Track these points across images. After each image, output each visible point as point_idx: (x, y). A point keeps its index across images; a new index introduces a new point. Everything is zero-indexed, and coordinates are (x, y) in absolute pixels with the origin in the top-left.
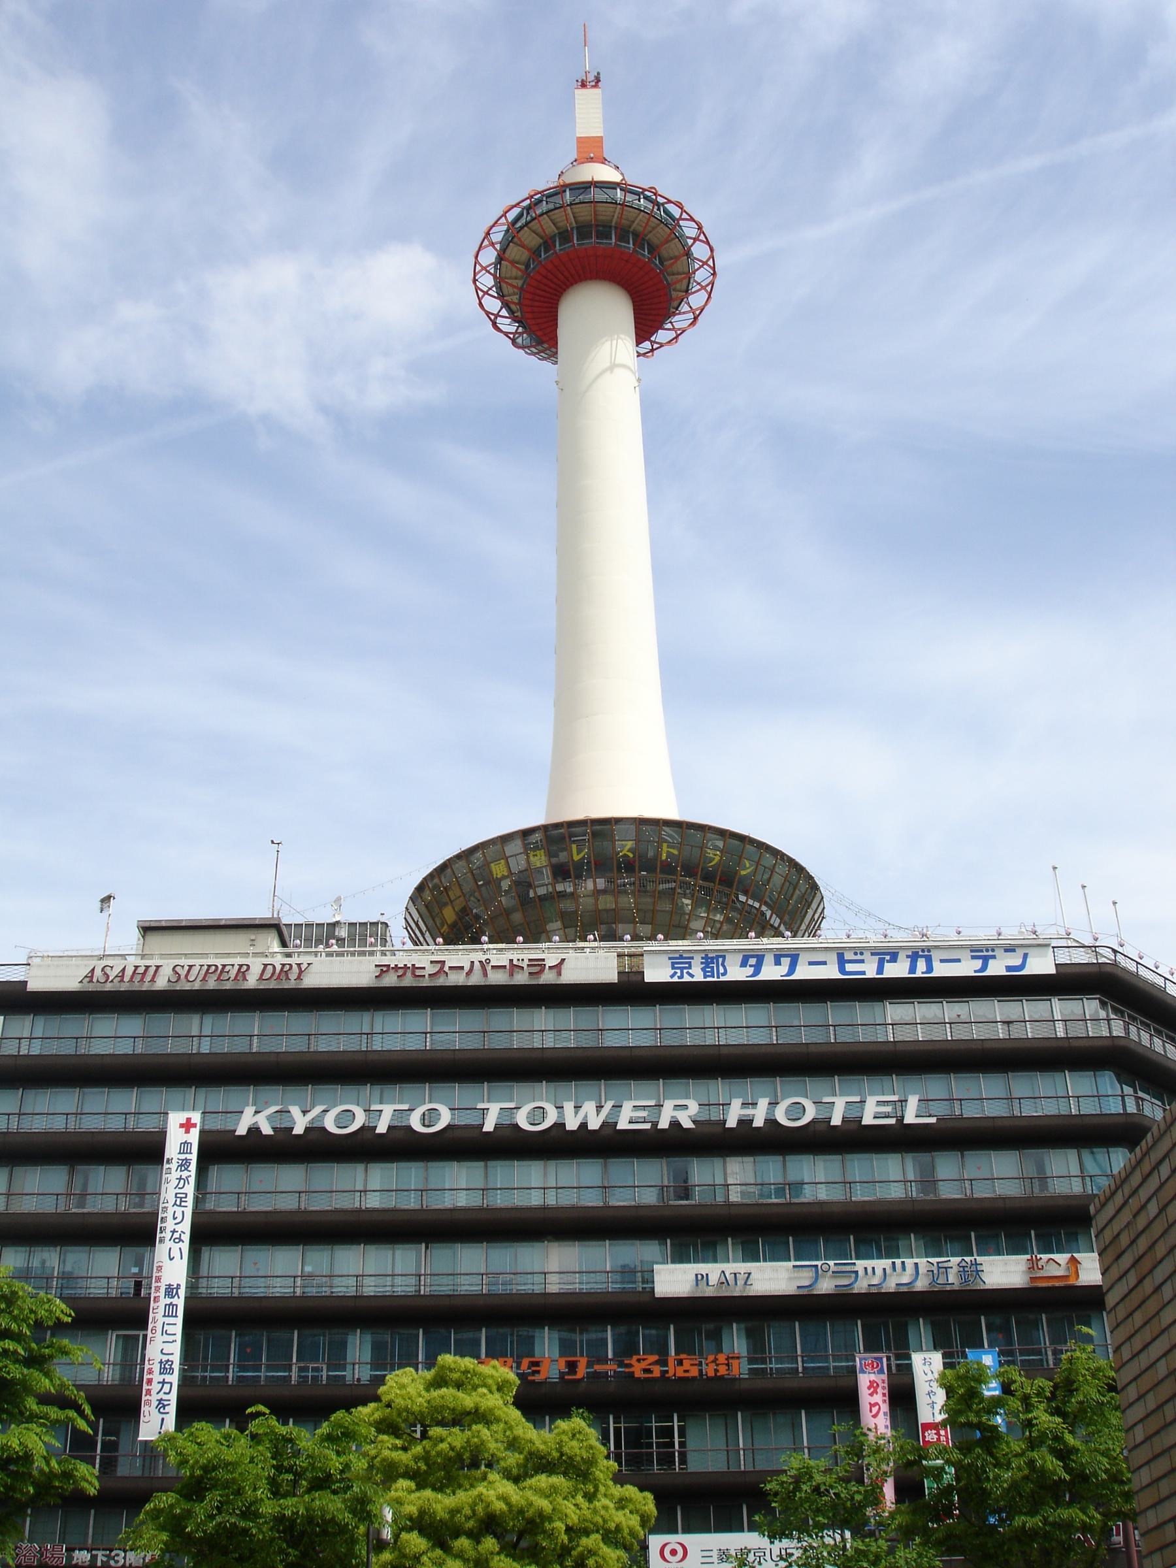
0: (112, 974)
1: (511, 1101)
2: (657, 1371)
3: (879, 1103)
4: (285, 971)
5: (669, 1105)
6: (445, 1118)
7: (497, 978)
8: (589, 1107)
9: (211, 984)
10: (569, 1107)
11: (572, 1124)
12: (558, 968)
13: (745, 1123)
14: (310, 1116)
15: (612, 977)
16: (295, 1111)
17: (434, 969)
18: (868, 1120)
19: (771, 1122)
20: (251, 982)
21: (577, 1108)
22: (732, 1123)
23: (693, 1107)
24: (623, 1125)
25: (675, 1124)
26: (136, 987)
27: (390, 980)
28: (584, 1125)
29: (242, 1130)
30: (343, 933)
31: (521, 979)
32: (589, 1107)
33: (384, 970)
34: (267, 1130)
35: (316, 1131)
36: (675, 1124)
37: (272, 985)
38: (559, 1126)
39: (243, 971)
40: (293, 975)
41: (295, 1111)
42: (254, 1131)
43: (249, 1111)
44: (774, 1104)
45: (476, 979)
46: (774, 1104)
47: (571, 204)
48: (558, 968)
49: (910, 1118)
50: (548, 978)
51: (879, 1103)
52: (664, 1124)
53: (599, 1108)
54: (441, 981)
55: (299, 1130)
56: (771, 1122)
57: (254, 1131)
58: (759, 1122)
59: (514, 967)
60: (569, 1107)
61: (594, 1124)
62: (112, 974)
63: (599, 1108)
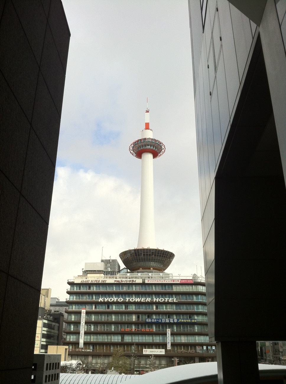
0: (84, 281)
1: (129, 298)
2: (145, 331)
3: (171, 299)
4: (104, 281)
5: (147, 299)
6: (122, 300)
7: (128, 282)
8: (138, 299)
9: (95, 282)
10: (136, 299)
11: (136, 301)
12: (135, 281)
13: (156, 301)
14: (107, 299)
15: (141, 282)
16: (105, 298)
18: (170, 301)
19: (159, 301)
20: (100, 282)
21: (137, 299)
22: (154, 301)
23: (150, 299)
24: (142, 301)
25: (148, 301)
26: (87, 283)
27: (116, 282)
28: (138, 301)
30: (111, 261)
31: (131, 282)
32: (138, 299)
33: (115, 281)
34: (102, 301)
35: (108, 301)
36: (148, 301)
37: (102, 283)
38: (135, 301)
39: (99, 281)
40: (105, 281)
41: (105, 298)
42: (101, 301)
43: (100, 298)
44: (159, 299)
45: (126, 282)
46: (159, 299)
47: (143, 142)
48: (135, 281)
50: (134, 282)
51: (171, 299)
52: (147, 301)
53: (139, 299)
54: (121, 283)
55: (106, 301)
56: (159, 301)
57: (101, 301)
58: (157, 301)
59: (130, 281)
60: (136, 299)
61: (139, 301)
62: (84, 281)
63: (139, 299)
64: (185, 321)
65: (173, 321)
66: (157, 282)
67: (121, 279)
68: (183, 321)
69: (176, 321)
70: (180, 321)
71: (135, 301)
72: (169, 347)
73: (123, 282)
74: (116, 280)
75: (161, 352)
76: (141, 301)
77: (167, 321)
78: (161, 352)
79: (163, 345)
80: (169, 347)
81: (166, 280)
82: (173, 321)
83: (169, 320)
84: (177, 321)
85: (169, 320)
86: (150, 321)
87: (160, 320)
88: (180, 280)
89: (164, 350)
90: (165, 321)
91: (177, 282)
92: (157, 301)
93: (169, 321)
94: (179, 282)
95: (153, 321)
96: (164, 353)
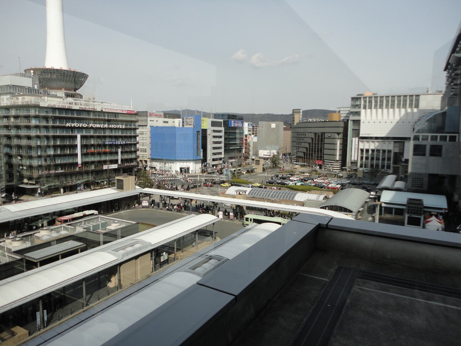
11: (97, 127)
13: (111, 127)
15: (100, 110)
16: (72, 124)
17: (84, 108)
19: (113, 127)
27: (80, 109)
29: (67, 126)
31: (93, 110)
33: (80, 108)
34: (70, 126)
38: (96, 127)
39: (65, 106)
42: (68, 126)
45: (89, 110)
49: (123, 128)
50: (95, 110)
55: (73, 126)
56: (113, 127)
57: (68, 126)
66: (112, 112)
67: (85, 106)
71: (96, 127)
72: (120, 162)
73: (87, 109)
74: (81, 107)
75: (115, 166)
76: (100, 127)
78: (115, 166)
79: (116, 162)
80: (120, 162)
81: (118, 110)
88: (126, 111)
89: (117, 165)
91: (125, 112)
92: (112, 127)
94: (126, 113)
96: (117, 167)
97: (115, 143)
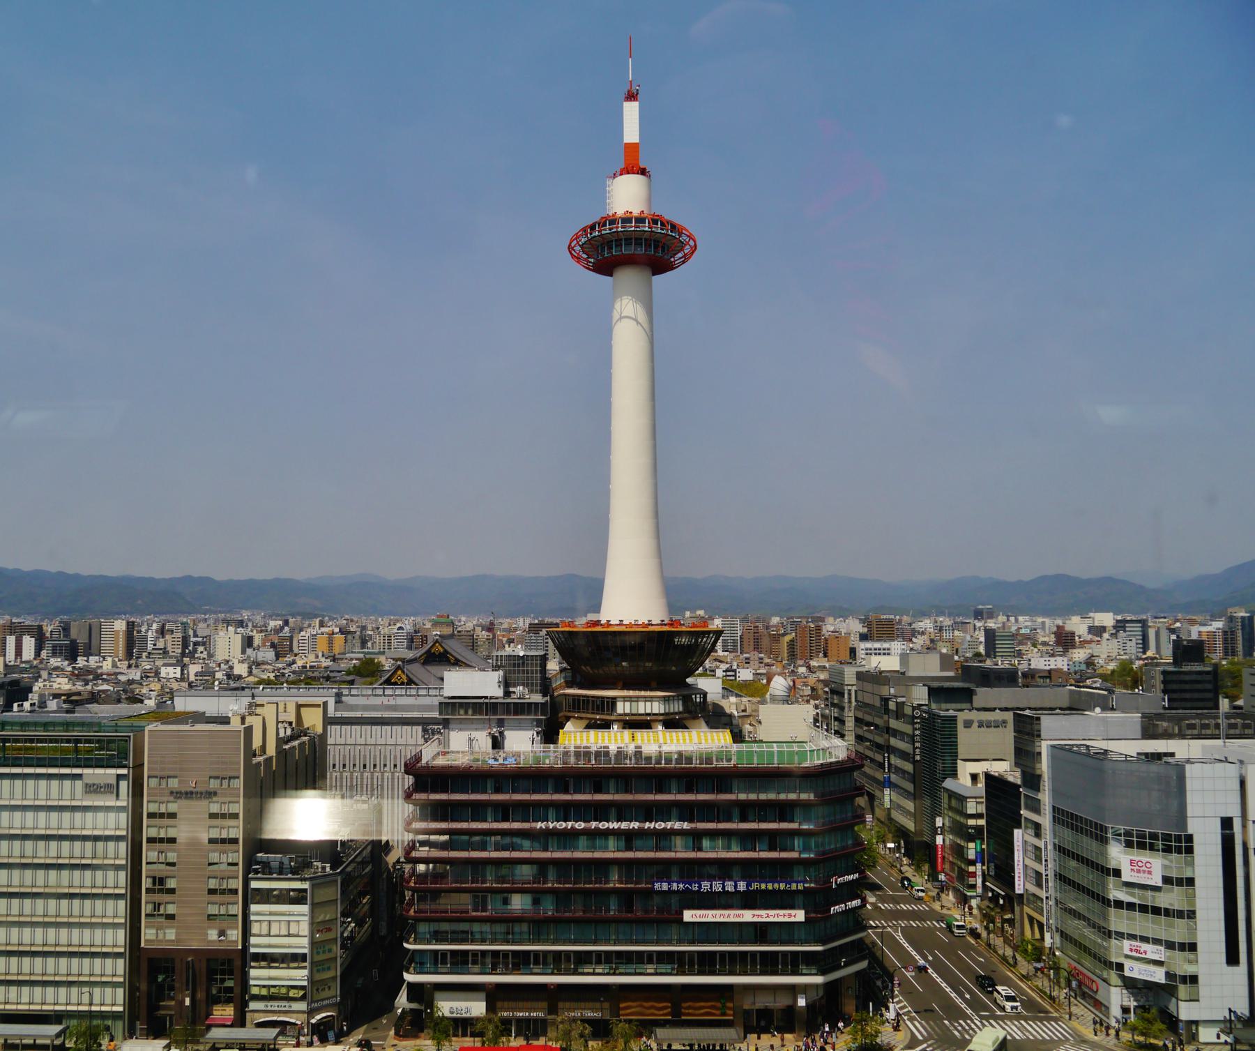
64: (770, 887)
65: (736, 887)
68: (763, 886)
69: (742, 886)
70: (755, 886)
77: (717, 887)
82: (736, 887)
83: (723, 884)
84: (747, 887)
85: (723, 884)
86: (665, 886)
87: (697, 885)
90: (711, 888)
93: (723, 888)
95: (674, 886)
97: (700, 887)
